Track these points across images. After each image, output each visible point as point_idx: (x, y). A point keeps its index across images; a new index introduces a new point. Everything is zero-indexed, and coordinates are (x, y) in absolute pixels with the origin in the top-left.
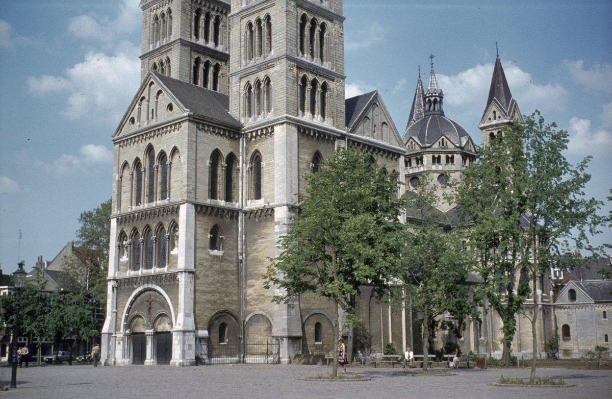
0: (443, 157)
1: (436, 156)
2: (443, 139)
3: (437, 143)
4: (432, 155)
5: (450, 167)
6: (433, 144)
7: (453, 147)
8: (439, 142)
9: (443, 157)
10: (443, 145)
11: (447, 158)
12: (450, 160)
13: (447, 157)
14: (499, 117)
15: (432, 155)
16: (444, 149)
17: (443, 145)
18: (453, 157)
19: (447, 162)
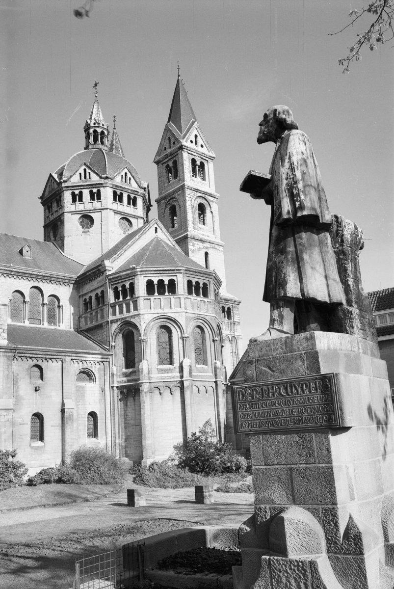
0: (86, 193)
1: (77, 192)
2: (85, 170)
3: (78, 174)
4: (71, 191)
5: (97, 205)
6: (71, 176)
7: (98, 178)
8: (80, 174)
9: (86, 193)
10: (85, 177)
11: (92, 193)
12: (96, 196)
13: (91, 192)
14: (174, 143)
15: (71, 191)
16: (86, 182)
17: (85, 177)
18: (99, 191)
19: (92, 198)
